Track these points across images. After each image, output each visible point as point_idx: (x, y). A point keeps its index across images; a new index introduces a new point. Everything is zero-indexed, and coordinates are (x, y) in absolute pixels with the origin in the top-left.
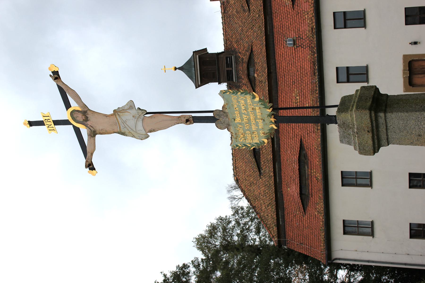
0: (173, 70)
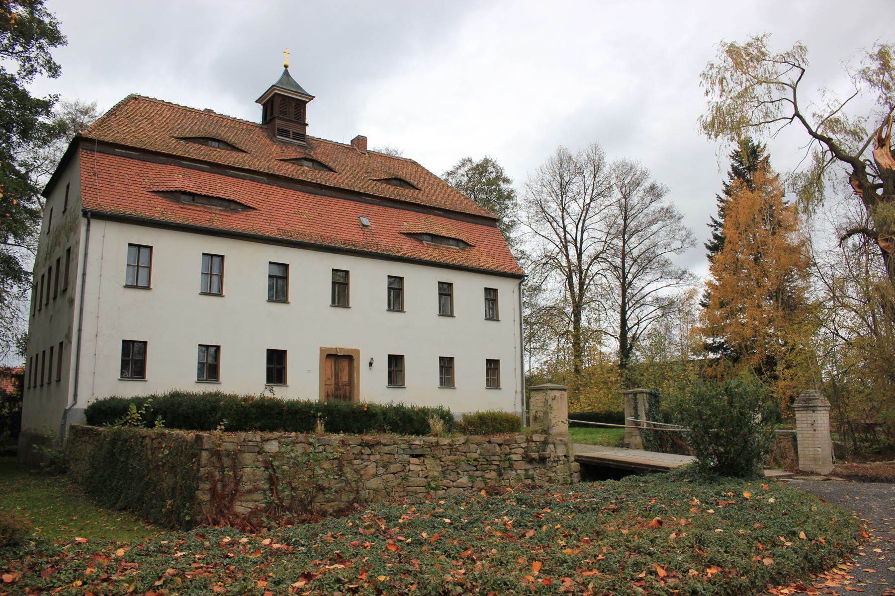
0: (285, 63)
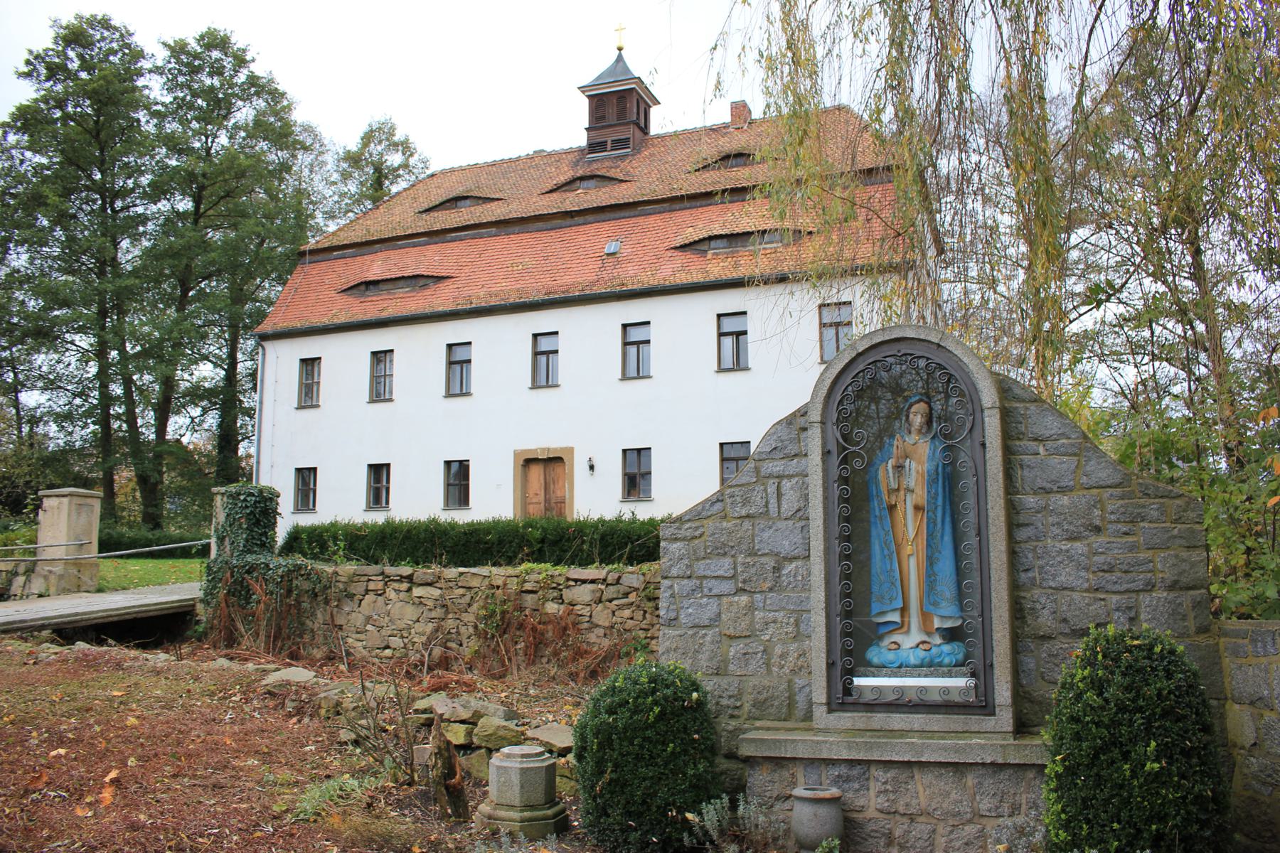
0: (619, 44)
